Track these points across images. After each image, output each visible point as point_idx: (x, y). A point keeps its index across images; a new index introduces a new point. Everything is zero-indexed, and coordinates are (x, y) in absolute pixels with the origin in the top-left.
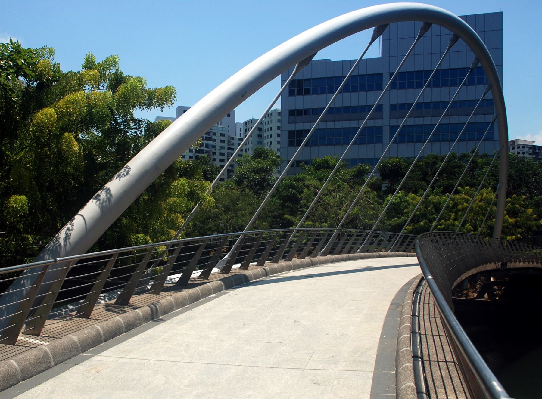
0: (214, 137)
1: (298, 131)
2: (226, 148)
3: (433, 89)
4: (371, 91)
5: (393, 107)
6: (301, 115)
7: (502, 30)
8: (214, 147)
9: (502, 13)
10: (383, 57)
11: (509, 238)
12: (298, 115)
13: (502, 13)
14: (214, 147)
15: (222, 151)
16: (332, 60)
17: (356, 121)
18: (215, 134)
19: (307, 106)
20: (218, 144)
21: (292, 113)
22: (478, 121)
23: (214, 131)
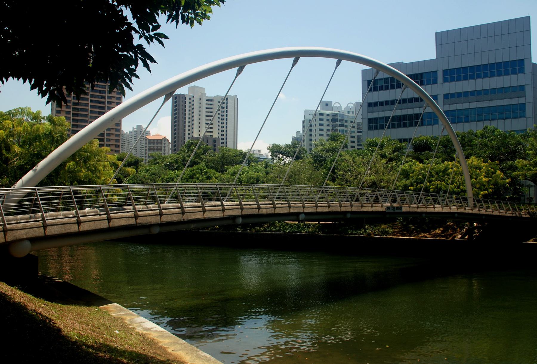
0: (346, 124)
1: (375, 119)
2: (356, 132)
3: (519, 75)
4: (429, 84)
5: (446, 96)
6: (377, 106)
7: (436, 45)
8: (346, 131)
9: (529, 17)
10: (437, 58)
11: (482, 193)
12: (386, 105)
13: (529, 17)
14: (346, 131)
15: (353, 134)
16: (405, 63)
17: (418, 109)
18: (346, 121)
19: (387, 99)
20: (349, 129)
21: (370, 105)
22: (512, 103)
23: (346, 119)
